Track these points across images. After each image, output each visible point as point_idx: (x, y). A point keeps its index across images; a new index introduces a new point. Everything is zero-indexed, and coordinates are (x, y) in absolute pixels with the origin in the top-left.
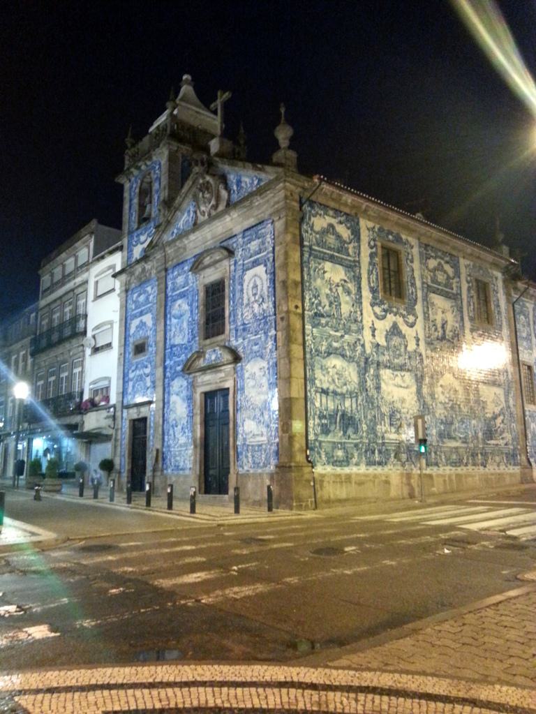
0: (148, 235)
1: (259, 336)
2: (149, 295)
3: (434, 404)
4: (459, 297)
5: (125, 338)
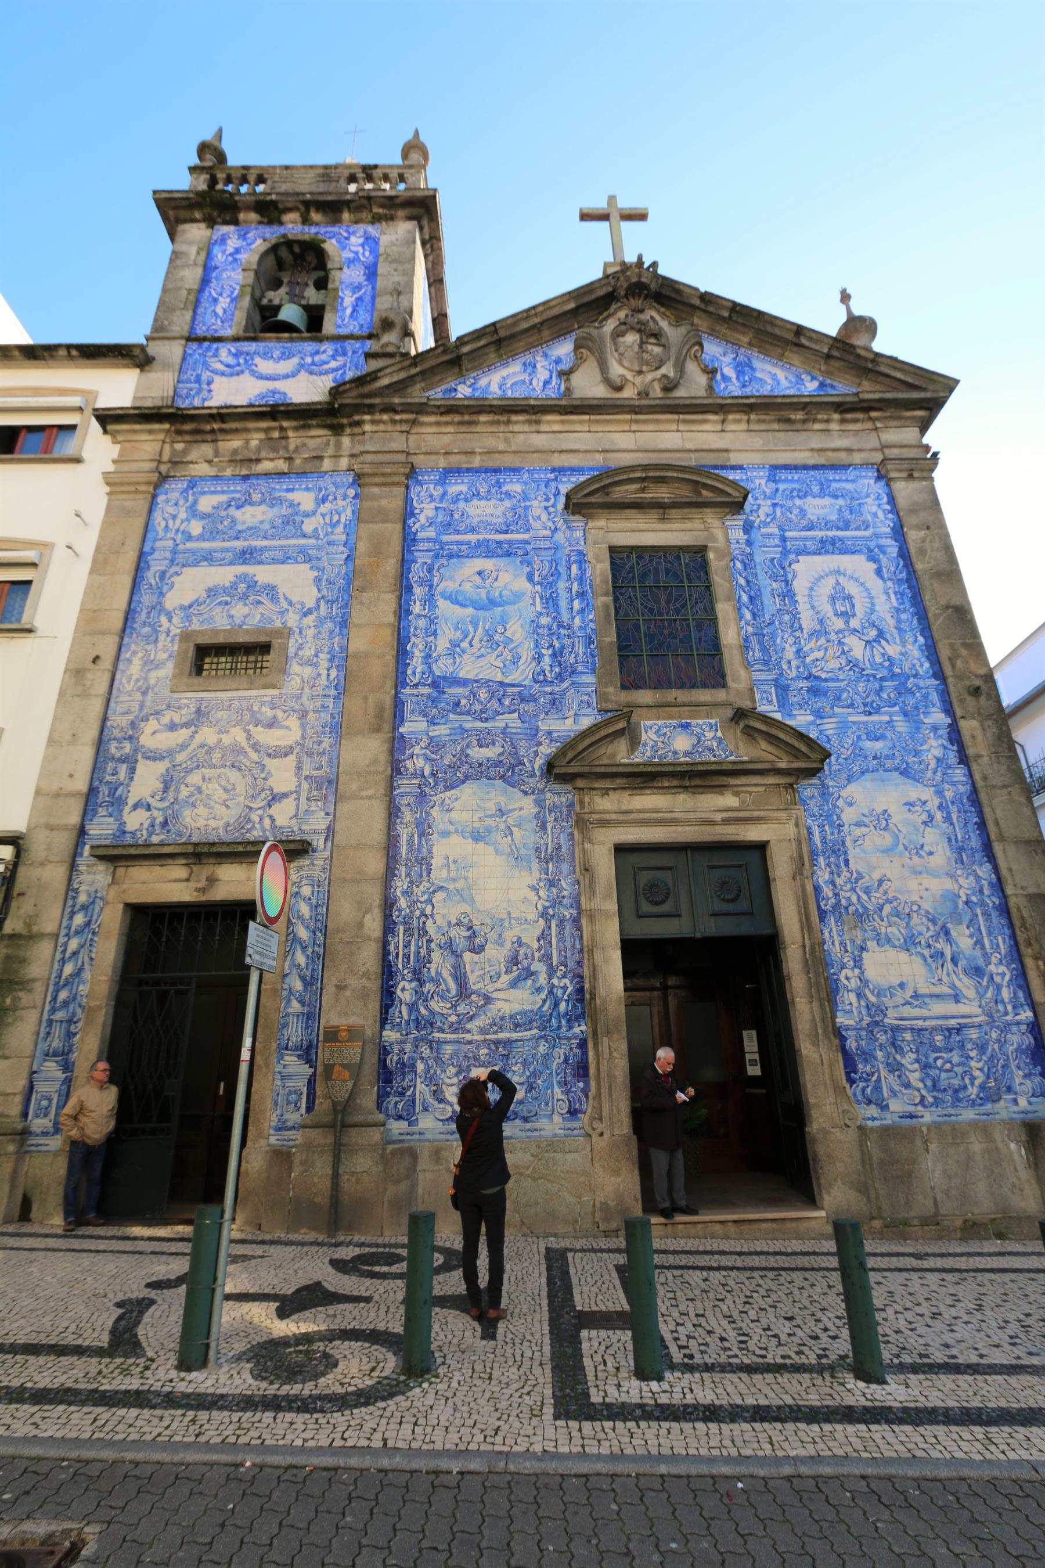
0: (302, 366)
1: (887, 718)
2: (307, 515)
5: (129, 615)
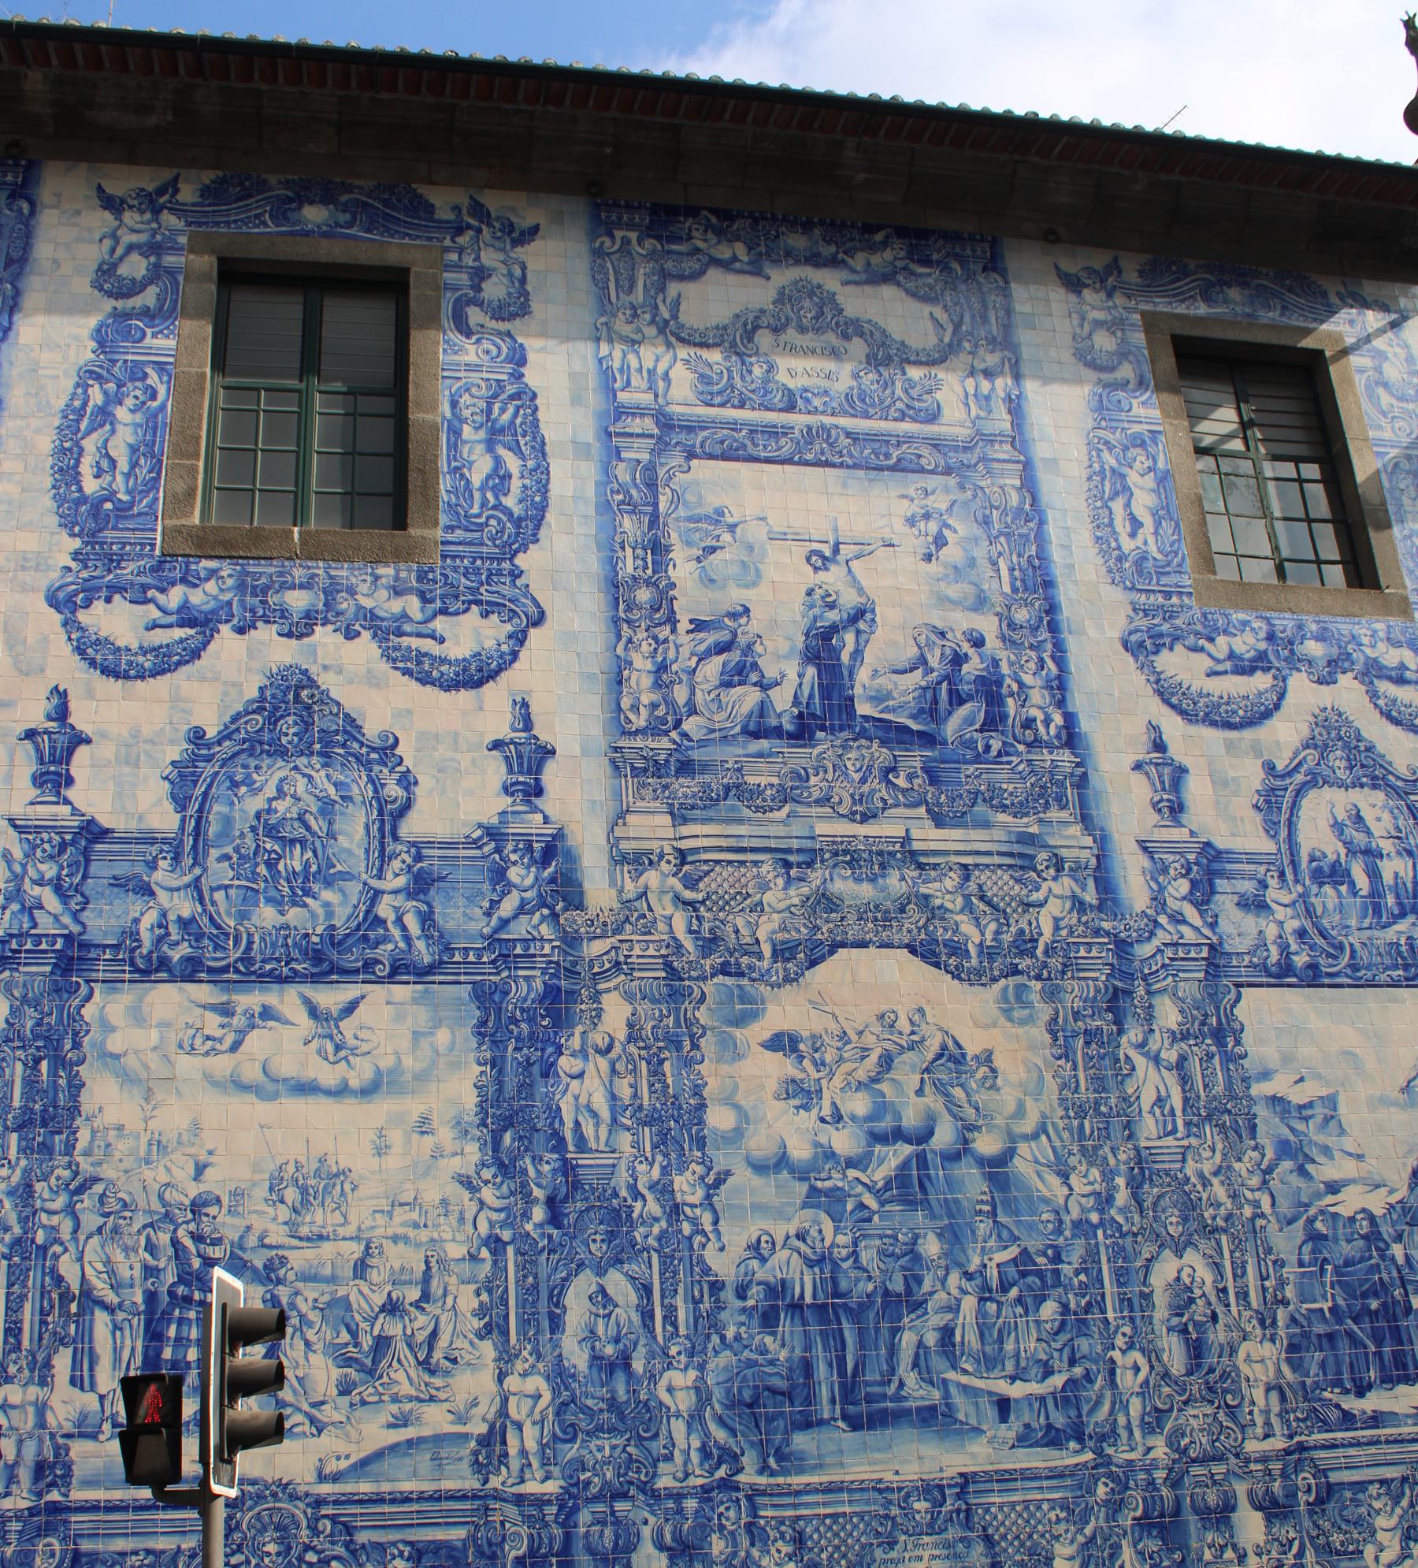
3: (680, 1182)
4: (1003, 451)
